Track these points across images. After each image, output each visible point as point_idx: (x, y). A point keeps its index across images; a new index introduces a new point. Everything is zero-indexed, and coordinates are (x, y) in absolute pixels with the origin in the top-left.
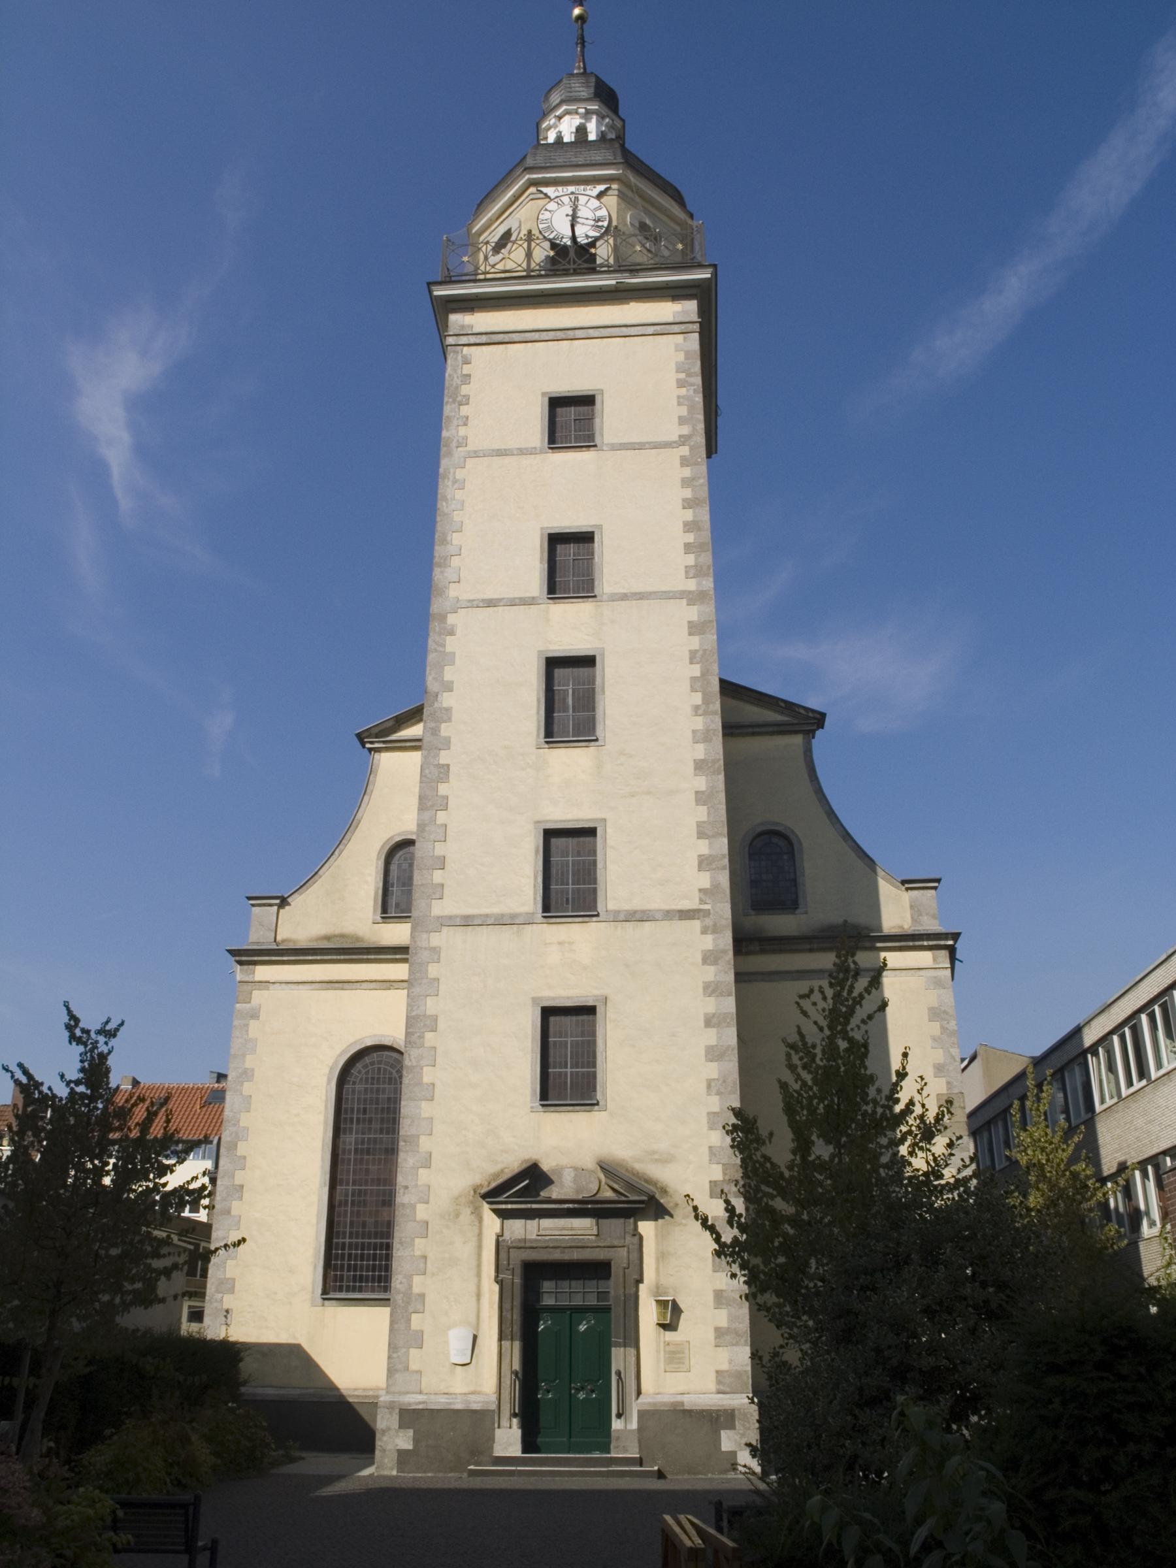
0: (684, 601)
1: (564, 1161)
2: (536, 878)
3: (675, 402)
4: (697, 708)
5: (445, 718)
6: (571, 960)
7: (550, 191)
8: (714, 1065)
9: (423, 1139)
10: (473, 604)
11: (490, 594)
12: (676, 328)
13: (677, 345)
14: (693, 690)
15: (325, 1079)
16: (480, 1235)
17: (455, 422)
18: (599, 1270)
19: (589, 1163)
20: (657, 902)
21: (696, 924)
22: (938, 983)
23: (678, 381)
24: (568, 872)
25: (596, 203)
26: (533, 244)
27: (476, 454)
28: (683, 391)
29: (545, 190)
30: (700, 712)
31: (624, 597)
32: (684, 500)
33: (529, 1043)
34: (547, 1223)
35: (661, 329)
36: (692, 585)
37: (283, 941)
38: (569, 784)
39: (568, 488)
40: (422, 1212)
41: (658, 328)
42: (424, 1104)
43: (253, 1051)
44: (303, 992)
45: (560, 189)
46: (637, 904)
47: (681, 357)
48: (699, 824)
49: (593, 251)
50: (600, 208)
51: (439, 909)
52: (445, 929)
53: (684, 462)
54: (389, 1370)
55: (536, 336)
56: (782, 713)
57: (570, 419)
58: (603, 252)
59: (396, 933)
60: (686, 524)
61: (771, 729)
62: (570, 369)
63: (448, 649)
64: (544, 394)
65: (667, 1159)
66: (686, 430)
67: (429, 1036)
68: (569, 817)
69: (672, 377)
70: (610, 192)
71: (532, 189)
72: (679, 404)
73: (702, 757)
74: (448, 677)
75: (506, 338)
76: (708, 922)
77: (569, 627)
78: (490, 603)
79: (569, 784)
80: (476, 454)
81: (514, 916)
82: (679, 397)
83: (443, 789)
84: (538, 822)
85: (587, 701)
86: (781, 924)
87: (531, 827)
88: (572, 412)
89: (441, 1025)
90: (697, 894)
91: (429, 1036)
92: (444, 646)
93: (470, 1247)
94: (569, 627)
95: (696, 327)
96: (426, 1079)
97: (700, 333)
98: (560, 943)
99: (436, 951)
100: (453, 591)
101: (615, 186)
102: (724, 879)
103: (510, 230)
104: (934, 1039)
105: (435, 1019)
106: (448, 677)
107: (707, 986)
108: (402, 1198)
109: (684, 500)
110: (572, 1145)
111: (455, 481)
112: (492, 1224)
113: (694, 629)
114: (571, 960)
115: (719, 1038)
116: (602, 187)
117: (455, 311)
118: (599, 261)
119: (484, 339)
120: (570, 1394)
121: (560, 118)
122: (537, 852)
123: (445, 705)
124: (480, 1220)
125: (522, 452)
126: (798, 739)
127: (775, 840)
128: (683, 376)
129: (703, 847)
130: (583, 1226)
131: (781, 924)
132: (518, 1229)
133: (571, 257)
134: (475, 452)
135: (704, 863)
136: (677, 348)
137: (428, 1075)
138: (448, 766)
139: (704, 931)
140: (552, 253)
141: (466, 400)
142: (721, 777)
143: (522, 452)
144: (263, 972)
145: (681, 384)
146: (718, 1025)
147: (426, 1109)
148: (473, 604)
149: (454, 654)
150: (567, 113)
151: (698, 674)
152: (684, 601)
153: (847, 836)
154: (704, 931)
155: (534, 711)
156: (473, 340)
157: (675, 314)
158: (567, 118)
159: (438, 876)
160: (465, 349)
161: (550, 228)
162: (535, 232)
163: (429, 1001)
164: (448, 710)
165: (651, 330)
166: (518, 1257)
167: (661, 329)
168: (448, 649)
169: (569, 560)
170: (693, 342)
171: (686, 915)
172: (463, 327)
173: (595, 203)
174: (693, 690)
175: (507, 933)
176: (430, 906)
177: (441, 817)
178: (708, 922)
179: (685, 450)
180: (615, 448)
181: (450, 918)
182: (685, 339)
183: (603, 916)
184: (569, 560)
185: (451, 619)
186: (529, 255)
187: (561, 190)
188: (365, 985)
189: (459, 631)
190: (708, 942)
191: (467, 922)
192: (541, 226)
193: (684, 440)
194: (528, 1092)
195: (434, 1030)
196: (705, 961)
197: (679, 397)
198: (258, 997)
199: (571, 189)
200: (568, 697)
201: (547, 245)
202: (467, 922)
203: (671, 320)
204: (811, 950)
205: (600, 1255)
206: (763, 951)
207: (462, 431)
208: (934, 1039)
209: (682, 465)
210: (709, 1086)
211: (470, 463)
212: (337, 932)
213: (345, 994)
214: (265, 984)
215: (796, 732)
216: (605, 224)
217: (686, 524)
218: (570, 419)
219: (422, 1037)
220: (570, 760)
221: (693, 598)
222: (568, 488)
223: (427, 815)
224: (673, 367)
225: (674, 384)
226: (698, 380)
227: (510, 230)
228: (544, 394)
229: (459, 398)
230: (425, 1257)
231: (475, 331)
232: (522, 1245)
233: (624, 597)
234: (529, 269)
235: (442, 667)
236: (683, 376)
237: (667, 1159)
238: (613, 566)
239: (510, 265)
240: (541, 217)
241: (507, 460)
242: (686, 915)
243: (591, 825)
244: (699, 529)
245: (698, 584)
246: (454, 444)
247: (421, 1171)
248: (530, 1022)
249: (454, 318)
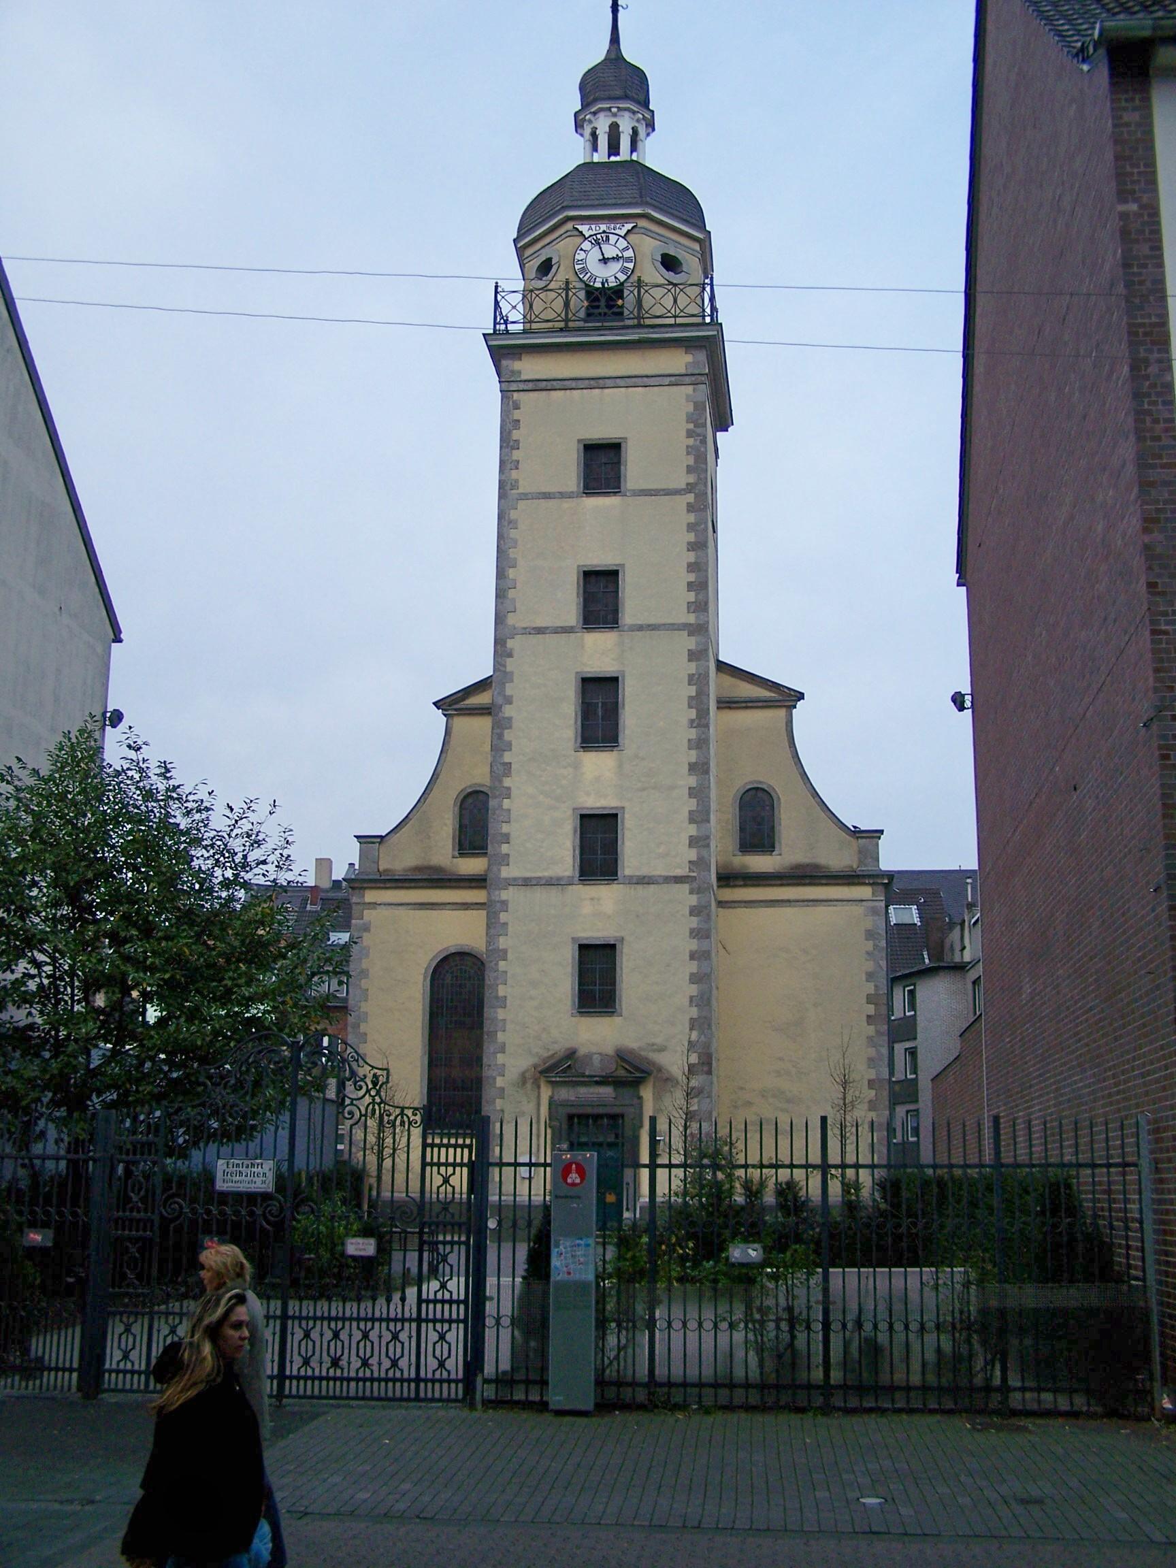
0: (685, 633)
1: (594, 1049)
4: (692, 721)
6: (598, 910)
7: (584, 228)
8: (694, 986)
9: (499, 1034)
11: (540, 622)
12: (687, 380)
14: (690, 707)
15: (421, 977)
16: (539, 1097)
17: (509, 466)
18: (615, 1118)
19: (610, 1051)
20: (659, 870)
21: (686, 887)
22: (874, 912)
23: (688, 431)
27: (525, 497)
28: (691, 441)
31: (640, 628)
32: (689, 543)
33: (569, 969)
34: (583, 1091)
35: (676, 380)
37: (385, 871)
38: (598, 779)
40: (500, 1082)
41: (673, 379)
42: (500, 1010)
43: (367, 956)
44: (401, 912)
46: (644, 871)
48: (690, 812)
49: (620, 302)
50: (626, 249)
51: (505, 872)
52: (511, 888)
55: (573, 384)
57: (602, 465)
58: (629, 299)
59: (472, 866)
62: (602, 416)
63: (508, 669)
64: (579, 441)
65: (662, 1049)
67: (502, 963)
68: (598, 805)
70: (636, 230)
71: (569, 226)
72: (688, 453)
73: (694, 760)
74: (508, 692)
75: (549, 385)
76: (695, 885)
77: (599, 652)
78: (540, 631)
79: (598, 779)
80: (525, 497)
81: (559, 879)
82: (688, 447)
83: (507, 782)
84: (574, 809)
85: (612, 711)
86: (760, 863)
87: (570, 812)
88: (603, 458)
89: (510, 956)
91: (502, 963)
92: (505, 666)
93: (532, 1105)
94: (599, 652)
96: (501, 994)
98: (592, 899)
99: (504, 903)
103: (550, 260)
104: (868, 953)
105: (505, 951)
106: (508, 692)
107: (692, 931)
108: (486, 1072)
109: (689, 543)
110: (598, 1036)
111: (510, 522)
112: (546, 1092)
114: (598, 910)
115: (699, 967)
116: (629, 226)
117: (506, 356)
118: (626, 312)
119: (530, 386)
121: (595, 113)
122: (575, 831)
123: (507, 715)
124: (539, 1087)
125: (563, 495)
126: (782, 713)
127: (760, 794)
128: (691, 426)
130: (607, 1091)
131: (760, 863)
132: (565, 1094)
133: (604, 303)
134: (525, 494)
137: (502, 990)
139: (691, 892)
143: (563, 495)
144: (370, 896)
146: (699, 959)
147: (501, 1014)
149: (512, 673)
150: (601, 110)
151: (694, 694)
153: (815, 794)
154: (691, 892)
155: (572, 722)
156: (522, 386)
158: (601, 115)
159: (505, 848)
160: (516, 395)
161: (584, 270)
162: (575, 284)
163: (501, 939)
164: (510, 719)
165: (667, 381)
166: (563, 1112)
167: (676, 380)
168: (508, 669)
170: (704, 390)
171: (678, 880)
172: (513, 372)
173: (622, 243)
174: (690, 707)
175: (554, 891)
176: (499, 870)
178: (695, 885)
179: (690, 498)
181: (515, 879)
183: (621, 880)
186: (567, 304)
188: (448, 907)
189: (515, 654)
190: (693, 900)
192: (577, 267)
194: (569, 1003)
195: (505, 959)
196: (691, 914)
197: (688, 447)
198: (368, 915)
199: (603, 227)
201: (582, 294)
202: (527, 883)
203: (683, 371)
204: (782, 885)
205: (616, 1110)
206: (745, 886)
208: (868, 953)
209: (688, 511)
210: (691, 1001)
211: (522, 505)
212: (426, 864)
213: (434, 913)
214: (374, 905)
216: (631, 266)
218: (602, 465)
219: (497, 964)
220: (598, 763)
225: (684, 434)
227: (550, 260)
228: (579, 441)
230: (503, 1111)
231: (524, 377)
232: (565, 1104)
234: (566, 320)
235: (504, 684)
236: (691, 426)
237: (662, 1049)
239: (550, 315)
240: (577, 257)
242: (678, 880)
243: (614, 812)
245: (697, 618)
246: (508, 487)
247: (499, 1055)
248: (569, 956)
249: (504, 363)
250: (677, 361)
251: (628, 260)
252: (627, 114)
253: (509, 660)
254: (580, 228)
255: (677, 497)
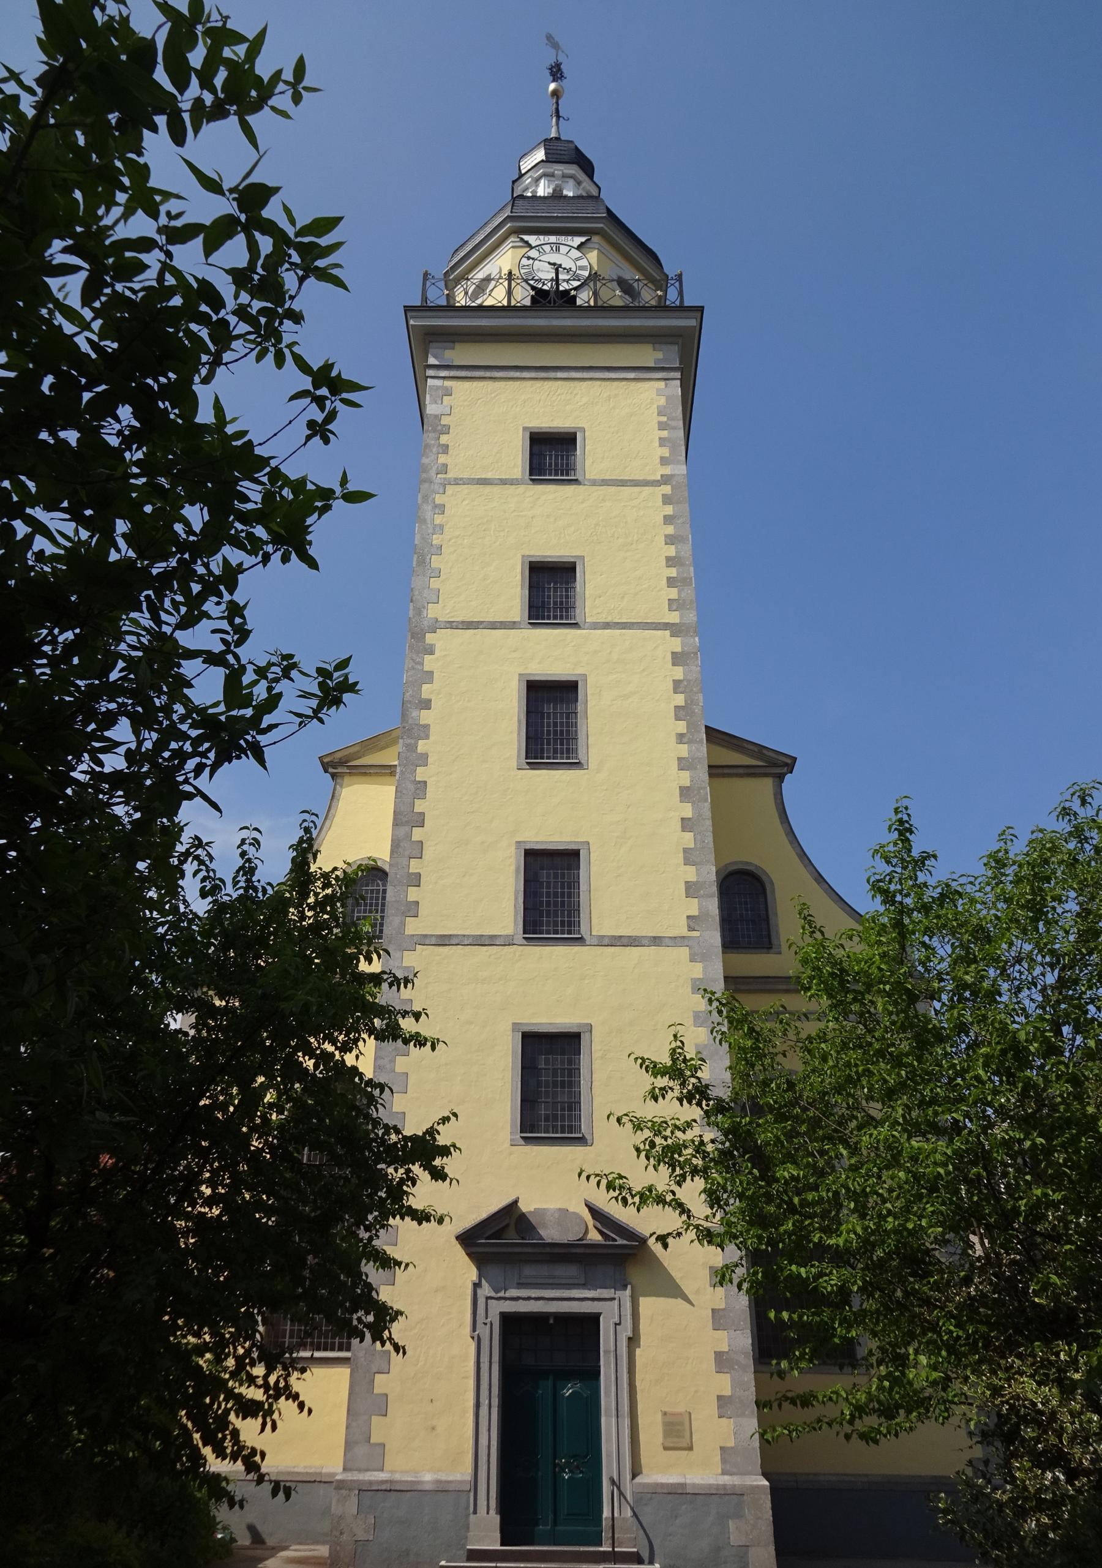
0: (668, 632)
2: (516, 898)
3: (657, 444)
5: (422, 735)
7: (532, 239)
10: (451, 625)
13: (658, 390)
17: (434, 450)
21: (685, 951)
23: (659, 423)
24: (551, 890)
25: (577, 254)
26: (513, 284)
27: (457, 482)
29: (526, 238)
30: (685, 740)
36: (674, 618)
38: (553, 807)
39: (551, 521)
45: (542, 237)
47: (662, 401)
53: (667, 500)
54: (346, 1442)
56: (752, 756)
57: (552, 454)
58: (584, 298)
60: (668, 559)
61: (741, 771)
64: (525, 429)
66: (667, 470)
69: (655, 419)
70: (589, 245)
77: (551, 653)
80: (457, 482)
90: (684, 922)
94: (551, 653)
95: (678, 375)
97: (681, 380)
100: (432, 612)
101: (596, 239)
102: (713, 906)
113: (677, 659)
116: (583, 239)
120: (554, 1472)
128: (664, 419)
129: (691, 874)
135: (691, 890)
136: (659, 393)
138: (425, 782)
140: (533, 293)
141: (446, 430)
142: (707, 805)
143: (504, 482)
145: (662, 426)
148: (451, 625)
152: (668, 632)
157: (656, 361)
169: (551, 589)
173: (576, 254)
174: (677, 718)
177: (417, 834)
179: (667, 489)
180: (594, 483)
182: (666, 385)
184: (551, 589)
185: (430, 638)
187: (543, 239)
191: (444, 941)
192: (522, 271)
193: (665, 480)
199: (553, 239)
200: (551, 719)
202: (444, 941)
207: (442, 459)
209: (665, 503)
215: (766, 775)
217: (668, 559)
218: (552, 454)
221: (675, 630)
222: (551, 521)
223: (402, 831)
224: (654, 410)
226: (680, 424)
228: (525, 429)
229: (439, 428)
233: (607, 626)
236: (664, 419)
238: (594, 593)
241: (487, 489)
244: (682, 565)
245: (681, 617)
250: (648, 355)
251: (582, 268)
252: (571, 182)
253: (427, 658)
254: (526, 238)
255: (647, 490)
